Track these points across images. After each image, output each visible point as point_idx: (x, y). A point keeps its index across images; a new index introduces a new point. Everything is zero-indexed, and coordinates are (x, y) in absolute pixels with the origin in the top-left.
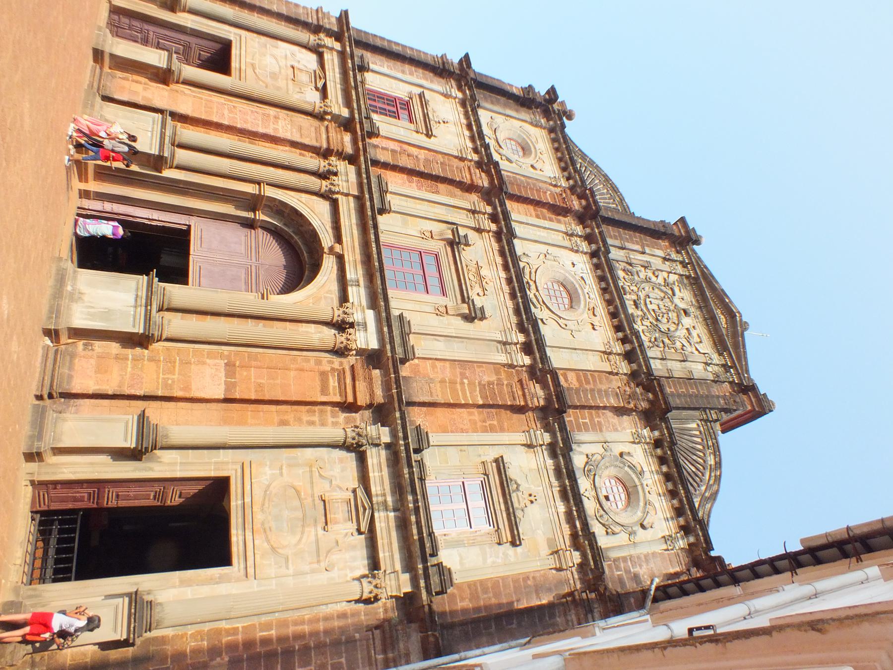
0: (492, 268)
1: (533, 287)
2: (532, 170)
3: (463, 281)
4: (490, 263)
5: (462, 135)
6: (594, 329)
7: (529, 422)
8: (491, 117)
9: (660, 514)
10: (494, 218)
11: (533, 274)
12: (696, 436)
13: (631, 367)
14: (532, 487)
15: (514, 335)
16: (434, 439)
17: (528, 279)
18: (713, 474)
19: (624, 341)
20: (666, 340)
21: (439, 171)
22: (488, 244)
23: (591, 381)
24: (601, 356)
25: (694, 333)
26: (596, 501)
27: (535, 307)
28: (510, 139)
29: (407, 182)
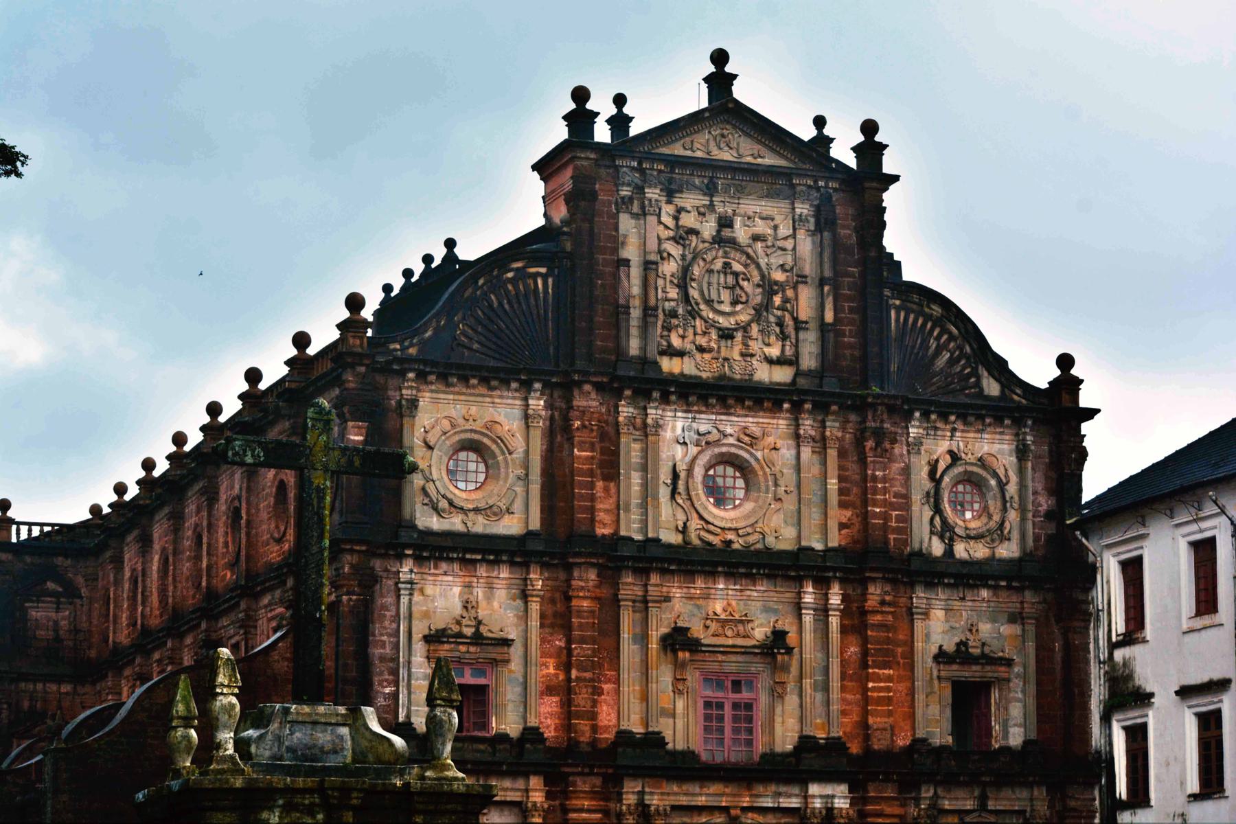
0: (712, 597)
1: (730, 536)
2: (514, 456)
3: (743, 650)
4: (705, 596)
8: (426, 504)
10: (643, 572)
11: (711, 528)
12: (906, 319)
14: (962, 623)
15: (807, 596)
16: (920, 734)
18: (953, 319)
19: (797, 408)
20: (777, 300)
21: (588, 649)
22: (678, 591)
25: (761, 227)
29: (603, 697)
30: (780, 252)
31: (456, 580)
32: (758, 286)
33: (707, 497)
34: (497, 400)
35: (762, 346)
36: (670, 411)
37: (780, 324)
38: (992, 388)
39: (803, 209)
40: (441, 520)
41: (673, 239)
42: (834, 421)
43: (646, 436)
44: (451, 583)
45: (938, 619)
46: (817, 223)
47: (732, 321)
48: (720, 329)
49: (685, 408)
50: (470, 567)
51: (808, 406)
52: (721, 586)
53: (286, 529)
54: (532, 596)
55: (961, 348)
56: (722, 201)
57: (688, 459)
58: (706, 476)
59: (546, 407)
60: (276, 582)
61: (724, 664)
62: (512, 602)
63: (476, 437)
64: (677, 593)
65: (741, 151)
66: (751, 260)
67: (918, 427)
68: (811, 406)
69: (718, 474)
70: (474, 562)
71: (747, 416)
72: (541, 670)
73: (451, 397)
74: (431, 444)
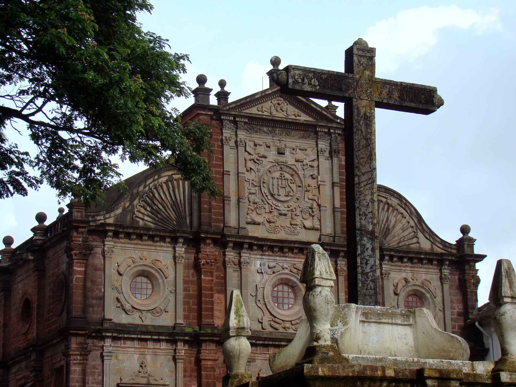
1: (288, 325)
2: (168, 279)
8: (119, 307)
22: (259, 356)
25: (300, 155)
30: (310, 168)
32: (299, 186)
33: (274, 303)
34: (158, 248)
35: (302, 219)
36: (254, 254)
37: (311, 208)
38: (426, 245)
39: (323, 145)
40: (127, 316)
42: (342, 261)
43: (241, 268)
44: (133, 353)
46: (330, 153)
47: (286, 205)
48: (279, 210)
49: (261, 253)
50: (143, 343)
53: (30, 326)
54: (179, 359)
55: (409, 222)
56: (279, 140)
57: (263, 281)
58: (273, 290)
59: (185, 252)
60: (23, 357)
62: (167, 363)
65: (289, 112)
66: (294, 173)
67: (387, 264)
69: (279, 290)
70: (146, 340)
71: (294, 258)
73: (133, 246)
74: (121, 273)
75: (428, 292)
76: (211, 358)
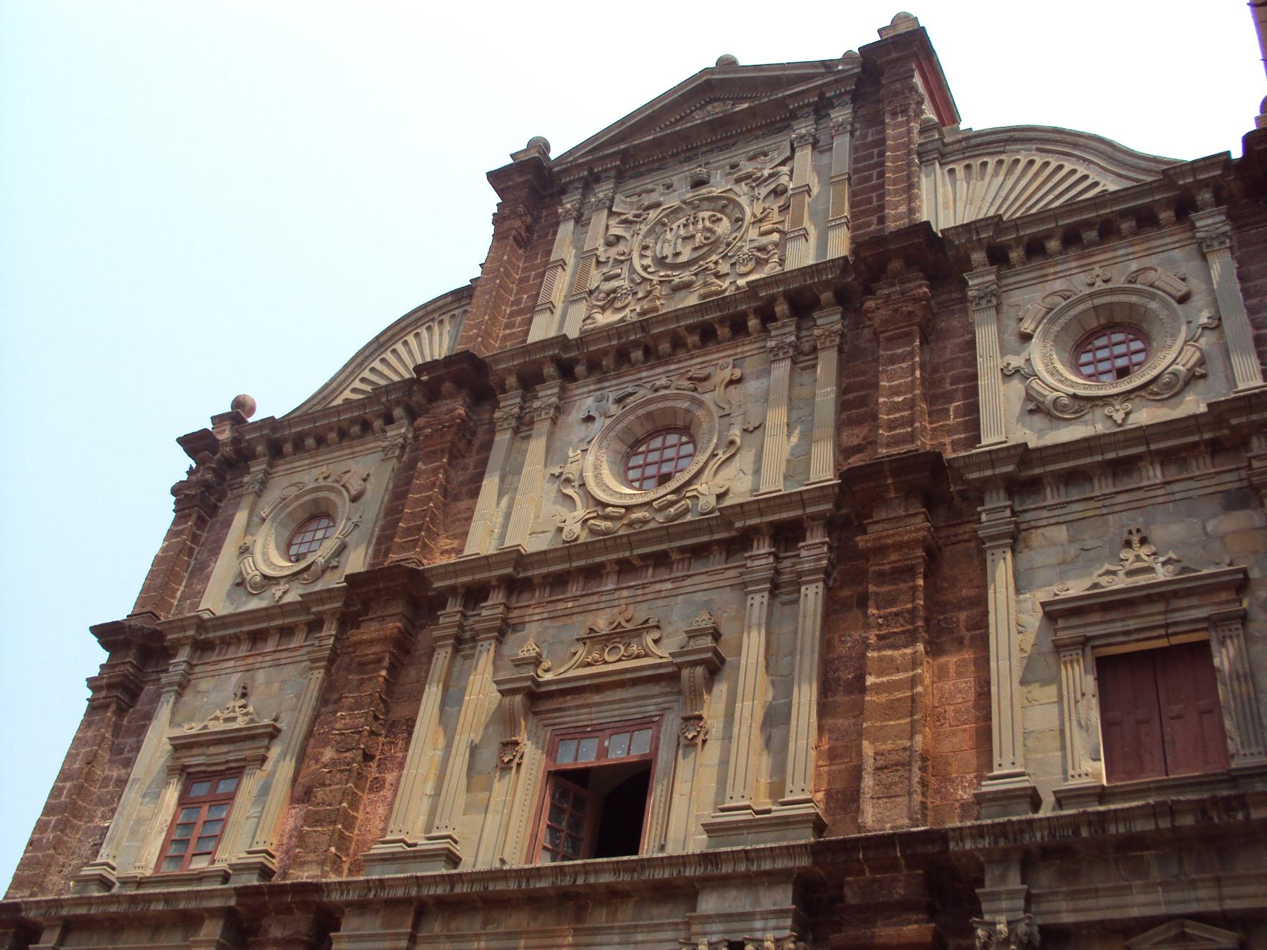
0: (594, 607)
2: (362, 501)
5: (277, 655)
6: (739, 381)
7: (960, 538)
9: (1153, 261)
13: (829, 305)
15: (757, 563)
17: (618, 524)
19: (767, 316)
22: (537, 611)
23: (862, 393)
24: (803, 369)
25: (747, 167)
26: (1132, 396)
27: (687, 511)
28: (289, 545)
31: (239, 663)
32: (738, 220)
34: (356, 449)
41: (625, 222)
45: (1053, 544)
48: (670, 282)
51: (781, 308)
52: (610, 587)
61: (594, 709)
63: (321, 494)
64: (536, 613)
68: (786, 306)
72: (309, 767)
73: (306, 462)
75: (1153, 297)
76: (374, 635)
